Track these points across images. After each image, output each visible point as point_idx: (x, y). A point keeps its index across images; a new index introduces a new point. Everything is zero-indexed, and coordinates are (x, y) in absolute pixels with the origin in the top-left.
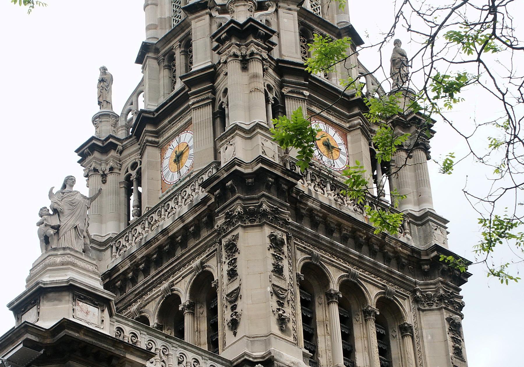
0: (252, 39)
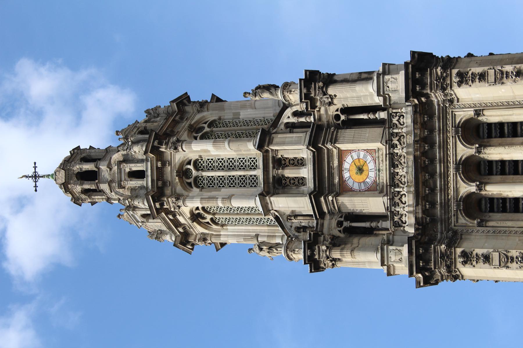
0: (317, 257)
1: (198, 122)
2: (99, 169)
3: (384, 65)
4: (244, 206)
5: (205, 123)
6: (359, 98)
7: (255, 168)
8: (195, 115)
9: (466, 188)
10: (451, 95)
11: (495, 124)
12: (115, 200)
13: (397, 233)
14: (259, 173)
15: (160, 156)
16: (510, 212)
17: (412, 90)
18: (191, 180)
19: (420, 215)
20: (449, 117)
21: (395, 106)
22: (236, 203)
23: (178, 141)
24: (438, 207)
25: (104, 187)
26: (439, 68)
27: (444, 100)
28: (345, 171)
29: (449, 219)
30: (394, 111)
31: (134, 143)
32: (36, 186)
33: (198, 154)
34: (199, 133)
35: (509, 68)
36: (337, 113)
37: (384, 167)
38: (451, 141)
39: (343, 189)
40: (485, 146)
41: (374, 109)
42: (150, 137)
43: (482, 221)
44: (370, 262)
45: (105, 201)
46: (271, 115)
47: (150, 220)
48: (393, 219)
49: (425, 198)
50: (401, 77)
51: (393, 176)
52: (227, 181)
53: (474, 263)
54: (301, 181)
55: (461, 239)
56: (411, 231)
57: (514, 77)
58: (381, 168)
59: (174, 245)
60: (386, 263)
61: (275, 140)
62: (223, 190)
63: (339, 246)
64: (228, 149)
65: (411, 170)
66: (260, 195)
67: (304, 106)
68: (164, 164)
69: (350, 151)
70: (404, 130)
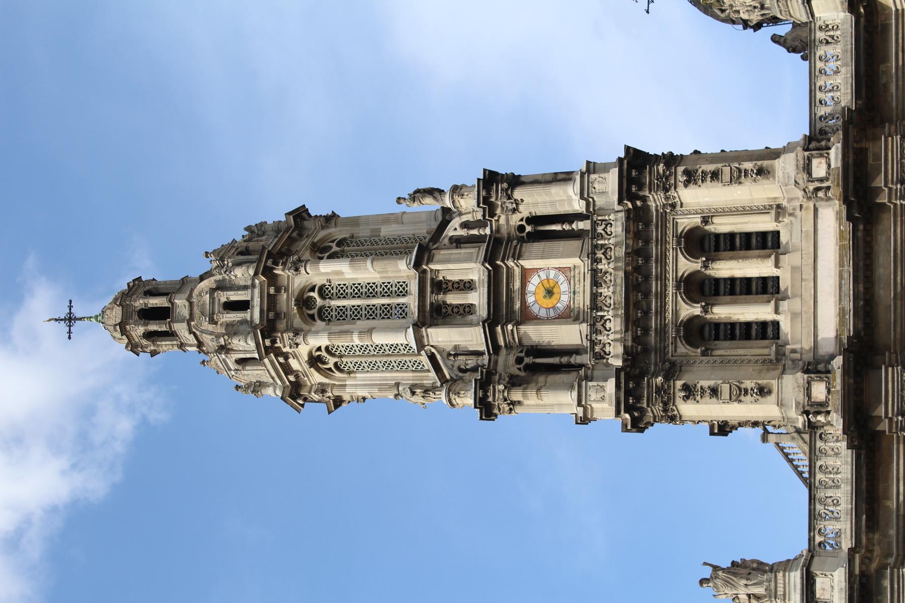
1: (322, 240)
2: (173, 304)
3: (588, 163)
4: (384, 343)
5: (333, 242)
6: (553, 203)
7: (404, 293)
8: (318, 232)
9: (689, 310)
10: (674, 198)
11: (725, 234)
12: (191, 346)
13: (597, 367)
14: (412, 301)
16: (740, 339)
17: (627, 191)
18: (314, 312)
19: (630, 343)
20: (670, 225)
21: (601, 212)
22: (379, 339)
23: (300, 260)
24: (653, 334)
26: (662, 165)
27: (664, 205)
28: (529, 295)
29: (665, 348)
30: (600, 218)
32: (70, 332)
33: (326, 278)
35: (748, 165)
36: (521, 223)
37: (582, 289)
38: (670, 255)
39: (526, 317)
40: (713, 260)
43: (707, 349)
44: (560, 405)
45: (176, 348)
46: (423, 230)
47: (247, 368)
48: (592, 349)
49: (636, 323)
50: (613, 177)
51: (594, 297)
52: (364, 312)
53: (698, 398)
54: (467, 310)
55: (681, 371)
56: (619, 363)
57: (754, 176)
58: (577, 290)
59: (282, 398)
60: (583, 403)
61: (436, 258)
62: (359, 322)
63: (520, 385)
64: (371, 269)
65: (621, 290)
66: (413, 325)
69: (536, 270)
70: (612, 241)
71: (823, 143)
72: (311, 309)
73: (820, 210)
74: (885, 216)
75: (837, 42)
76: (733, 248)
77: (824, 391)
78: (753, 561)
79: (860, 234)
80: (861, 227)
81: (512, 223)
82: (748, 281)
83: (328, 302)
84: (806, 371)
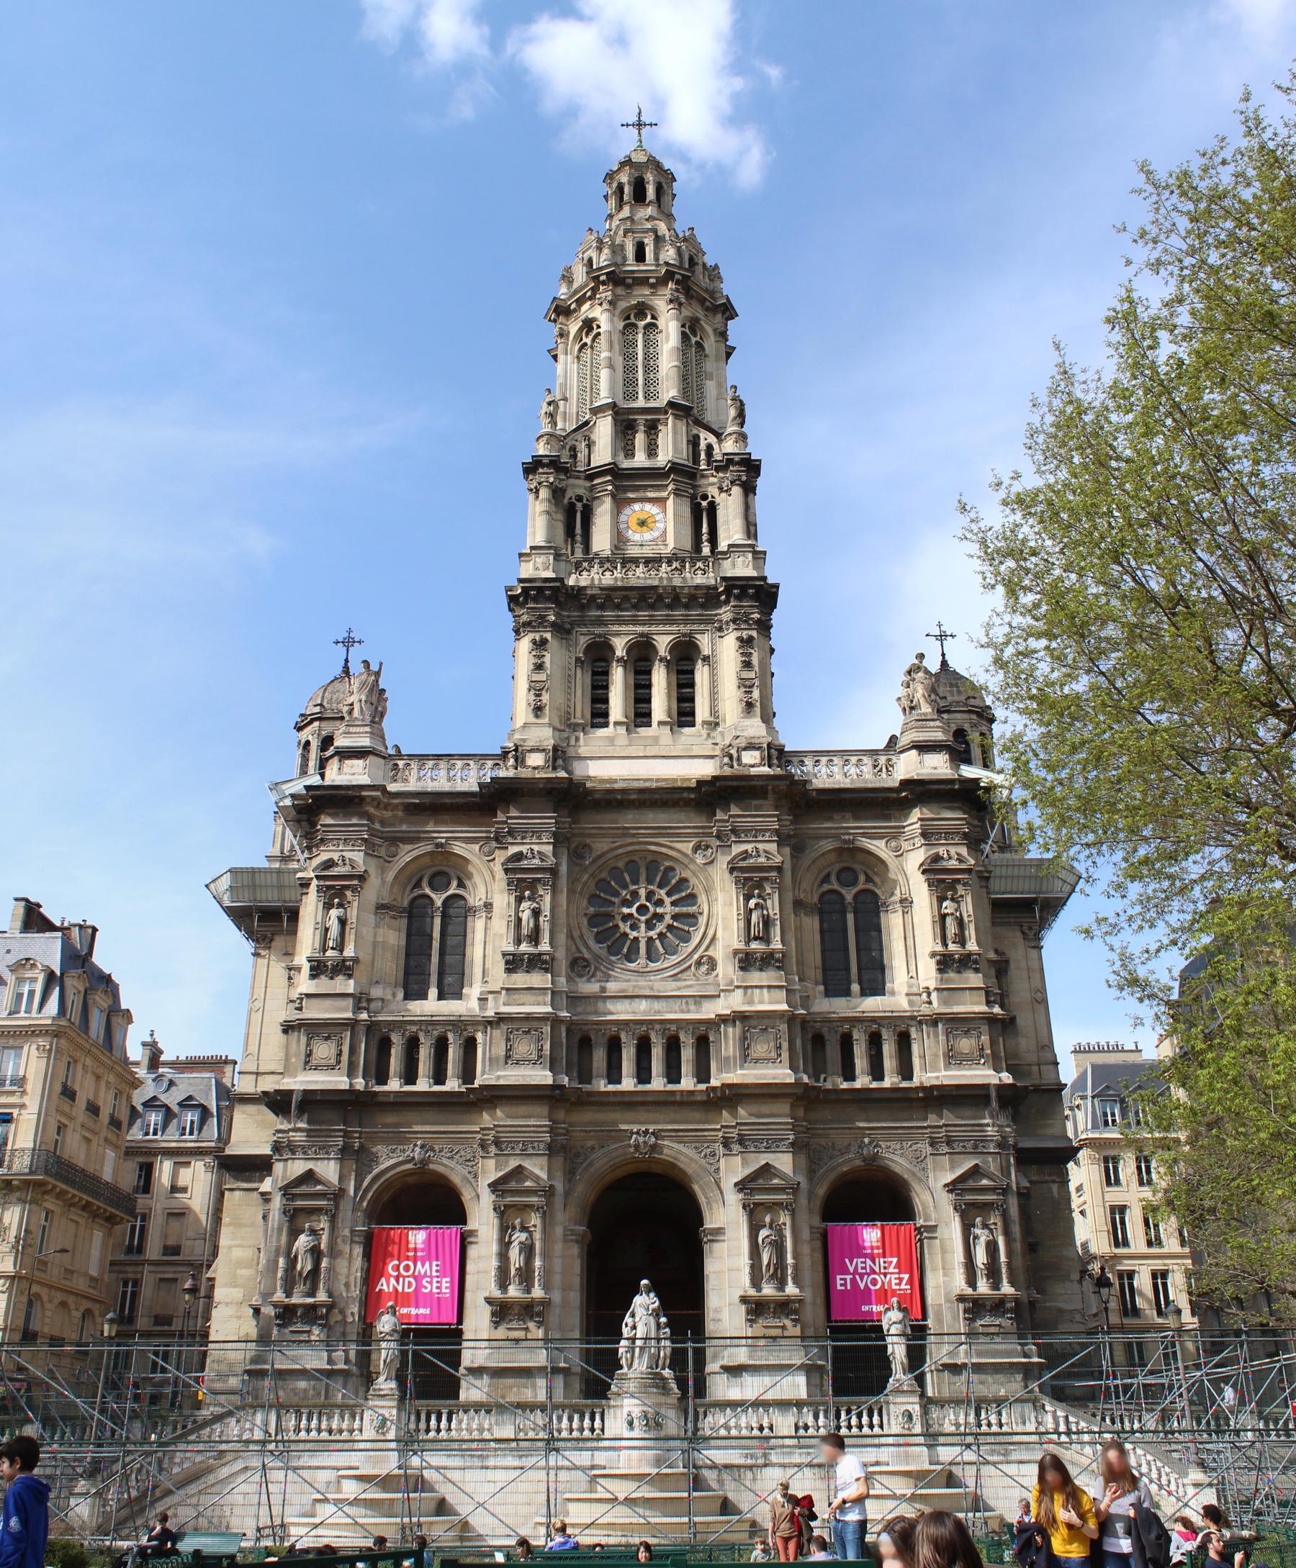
1: (702, 329)
3: (765, 553)
6: (727, 522)
9: (620, 646)
14: (640, 403)
15: (663, 281)
18: (633, 320)
19: (589, 592)
20: (702, 627)
22: (604, 374)
23: (680, 304)
24: (599, 613)
25: (626, 211)
29: (585, 625)
31: (679, 250)
34: (690, 330)
35: (756, 694)
38: (674, 628)
39: (620, 503)
40: (667, 667)
41: (713, 540)
42: (685, 269)
43: (582, 662)
44: (534, 533)
46: (709, 417)
49: (609, 598)
50: (750, 572)
51: (635, 561)
56: (571, 581)
61: (679, 423)
62: (621, 359)
65: (641, 583)
67: (719, 458)
68: (653, 286)
71: (775, 761)
72: (635, 317)
73: (712, 761)
74: (704, 818)
75: (875, 775)
76: (680, 686)
77: (535, 764)
78: (385, 708)
79: (685, 795)
80: (692, 796)
81: (710, 489)
82: (648, 700)
83: (641, 331)
84: (555, 749)
